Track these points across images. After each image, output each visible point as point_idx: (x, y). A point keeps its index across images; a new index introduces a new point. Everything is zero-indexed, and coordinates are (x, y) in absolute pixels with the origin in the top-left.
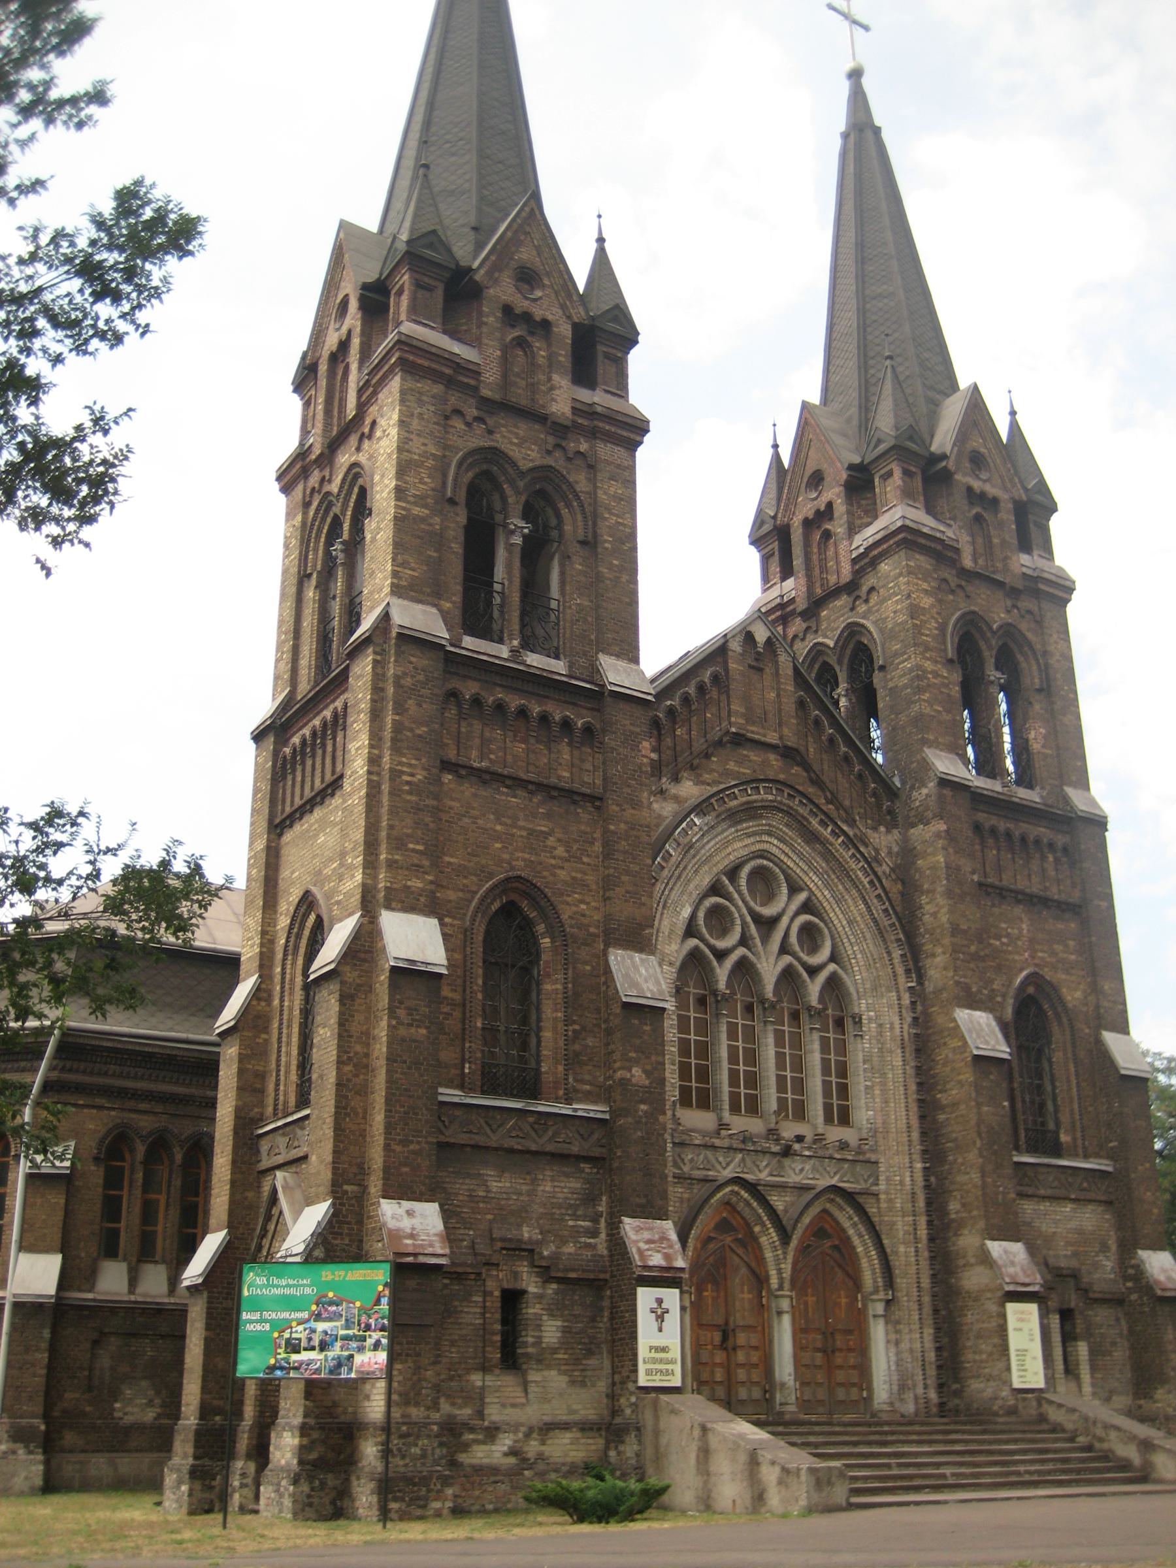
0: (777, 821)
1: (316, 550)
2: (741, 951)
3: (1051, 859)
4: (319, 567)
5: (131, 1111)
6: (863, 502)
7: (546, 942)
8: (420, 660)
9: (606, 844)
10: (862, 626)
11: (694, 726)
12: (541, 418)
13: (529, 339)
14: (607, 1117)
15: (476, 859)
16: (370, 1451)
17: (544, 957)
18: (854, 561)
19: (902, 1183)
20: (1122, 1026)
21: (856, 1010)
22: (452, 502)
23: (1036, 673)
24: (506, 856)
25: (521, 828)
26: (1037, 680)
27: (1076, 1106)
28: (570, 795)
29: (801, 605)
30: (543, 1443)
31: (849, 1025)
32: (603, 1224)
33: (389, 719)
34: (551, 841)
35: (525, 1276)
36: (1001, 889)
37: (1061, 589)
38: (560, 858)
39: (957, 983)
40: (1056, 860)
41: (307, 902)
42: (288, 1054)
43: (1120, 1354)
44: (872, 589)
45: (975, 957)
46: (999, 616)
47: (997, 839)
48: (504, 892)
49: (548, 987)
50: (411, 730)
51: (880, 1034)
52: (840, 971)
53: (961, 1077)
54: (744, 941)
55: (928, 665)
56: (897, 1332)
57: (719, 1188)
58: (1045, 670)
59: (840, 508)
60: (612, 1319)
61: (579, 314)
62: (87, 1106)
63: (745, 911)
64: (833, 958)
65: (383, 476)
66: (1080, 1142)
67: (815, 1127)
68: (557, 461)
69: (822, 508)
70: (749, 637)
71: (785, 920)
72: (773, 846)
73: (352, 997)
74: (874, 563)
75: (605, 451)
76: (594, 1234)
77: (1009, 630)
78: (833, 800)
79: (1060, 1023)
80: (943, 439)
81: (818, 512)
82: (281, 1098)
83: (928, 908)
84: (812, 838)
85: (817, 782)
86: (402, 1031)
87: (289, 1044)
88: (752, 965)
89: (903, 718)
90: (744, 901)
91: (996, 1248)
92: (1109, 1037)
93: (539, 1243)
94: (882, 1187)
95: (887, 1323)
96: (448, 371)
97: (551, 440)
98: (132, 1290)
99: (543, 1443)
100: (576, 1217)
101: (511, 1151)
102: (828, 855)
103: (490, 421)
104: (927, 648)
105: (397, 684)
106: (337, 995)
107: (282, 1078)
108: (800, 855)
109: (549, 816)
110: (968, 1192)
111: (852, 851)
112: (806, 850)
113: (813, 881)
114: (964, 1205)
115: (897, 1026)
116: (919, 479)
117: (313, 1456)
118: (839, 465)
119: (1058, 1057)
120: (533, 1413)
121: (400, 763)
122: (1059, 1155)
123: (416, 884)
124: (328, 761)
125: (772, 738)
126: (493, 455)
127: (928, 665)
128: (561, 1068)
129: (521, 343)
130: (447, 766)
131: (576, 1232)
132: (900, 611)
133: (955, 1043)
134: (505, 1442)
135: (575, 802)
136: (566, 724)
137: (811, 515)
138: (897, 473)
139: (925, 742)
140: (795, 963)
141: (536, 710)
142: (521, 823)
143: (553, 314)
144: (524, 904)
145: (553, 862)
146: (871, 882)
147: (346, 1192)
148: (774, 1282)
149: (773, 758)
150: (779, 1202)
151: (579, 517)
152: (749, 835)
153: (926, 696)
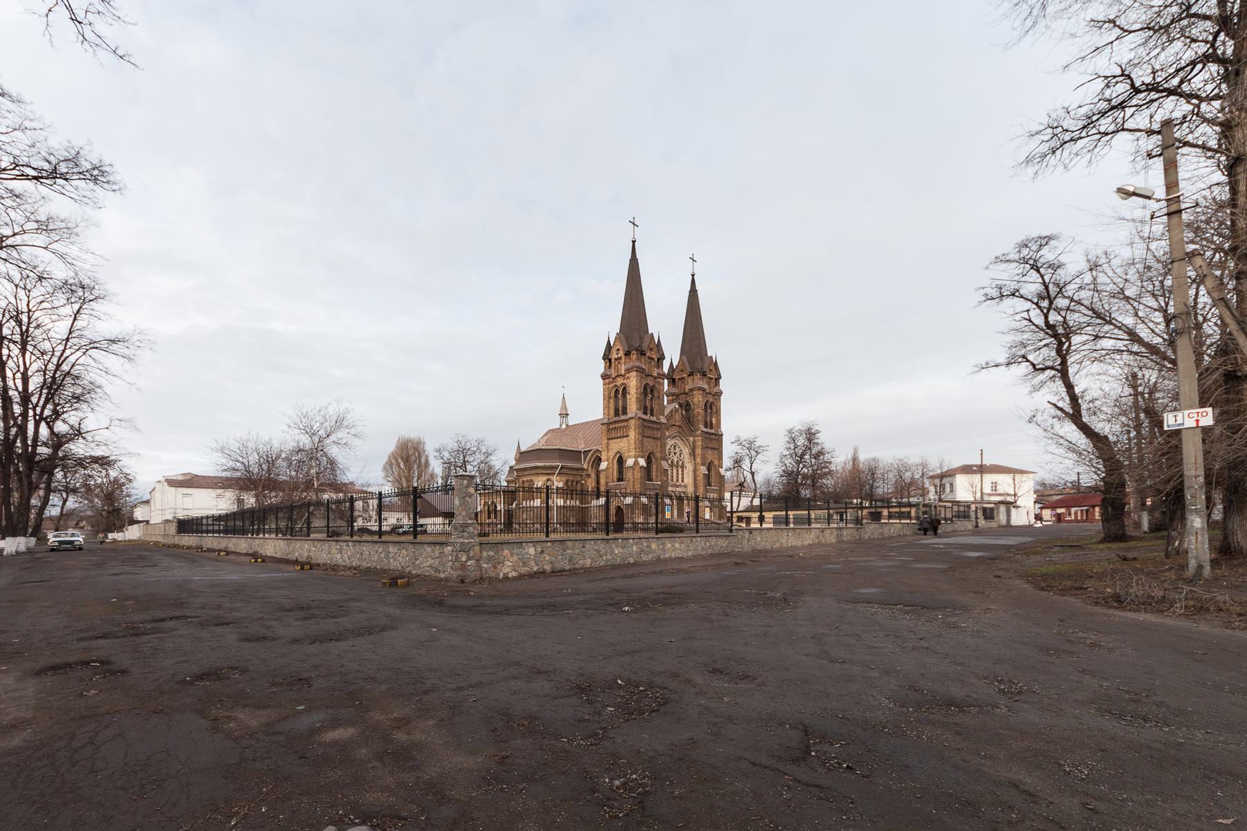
0: (678, 438)
28: (657, 439)
41: (618, 452)
61: (658, 357)
84: (682, 440)
113: (682, 446)
125: (677, 424)
143: (654, 356)
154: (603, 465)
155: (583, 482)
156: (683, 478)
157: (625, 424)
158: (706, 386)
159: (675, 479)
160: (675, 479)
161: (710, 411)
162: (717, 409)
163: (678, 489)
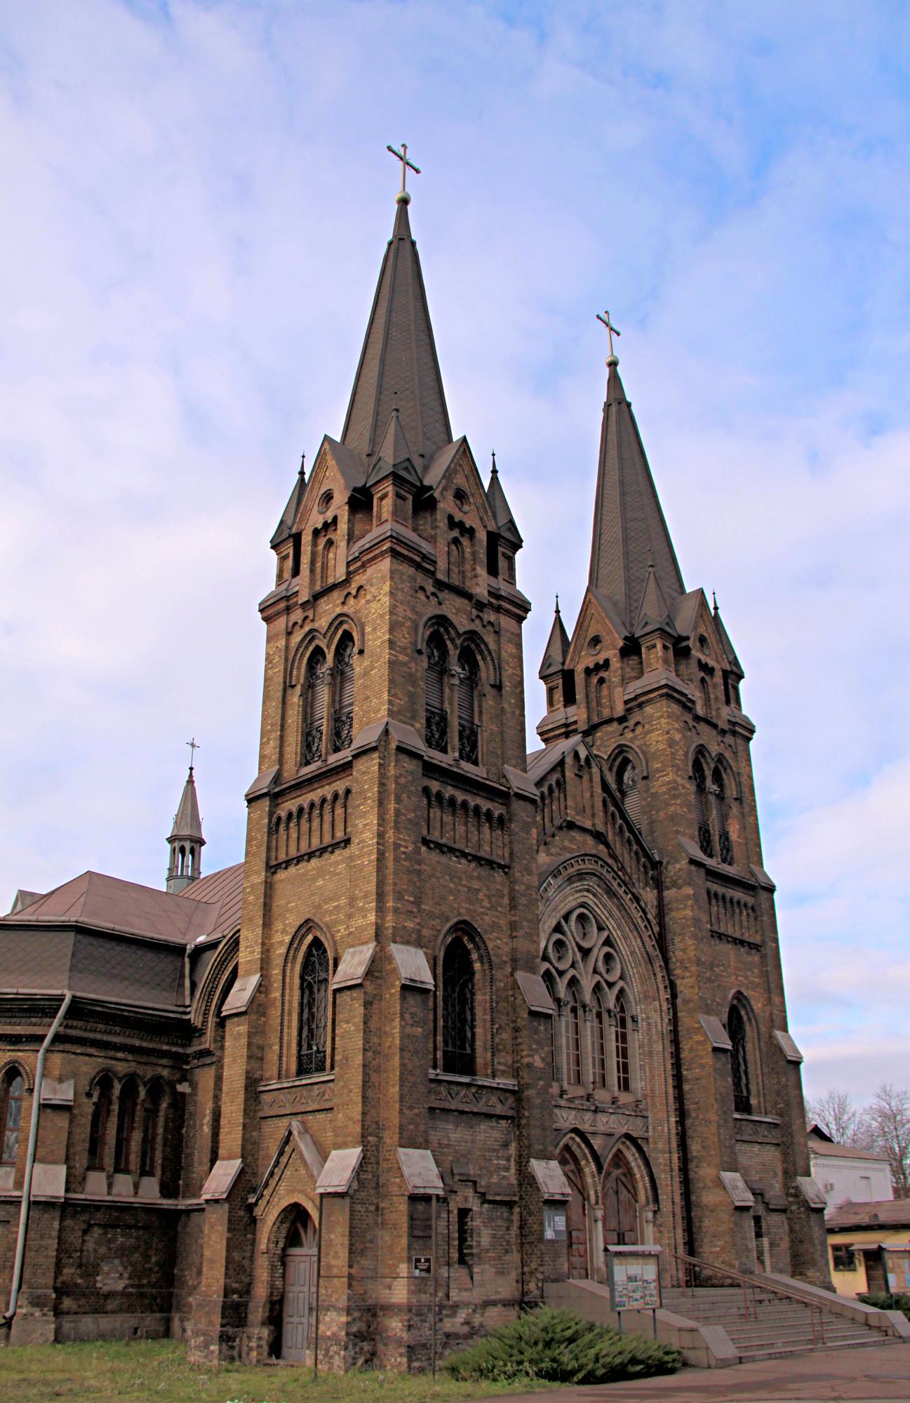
0: (592, 882)
1: (299, 669)
2: (571, 972)
3: (745, 913)
4: (302, 681)
5: (112, 1058)
6: (631, 662)
7: (477, 966)
8: (411, 766)
9: (512, 899)
10: (631, 748)
11: (546, 815)
12: (468, 596)
13: (461, 539)
14: (516, 1088)
15: (438, 907)
16: (395, 1325)
17: (478, 976)
18: (626, 702)
19: (662, 1131)
20: (785, 1028)
21: (634, 1013)
22: (420, 652)
23: (734, 787)
24: (456, 906)
25: (465, 886)
26: (735, 792)
27: (760, 1080)
28: (491, 864)
29: (582, 726)
30: (482, 1315)
31: (629, 1021)
32: (513, 1162)
33: (392, 806)
34: (481, 896)
35: (471, 1199)
36: (721, 934)
37: (744, 731)
38: (487, 908)
39: (700, 998)
40: (748, 914)
41: (307, 925)
42: (289, 1034)
43: (785, 1245)
44: (637, 723)
45: (709, 980)
46: (714, 749)
47: (717, 900)
48: (456, 931)
49: (479, 997)
50: (405, 815)
51: (649, 1029)
52: (626, 987)
53: (703, 1061)
54: (573, 966)
55: (679, 779)
56: (660, 1232)
57: (565, 1135)
58: (739, 785)
59: (615, 663)
60: (521, 1227)
61: (492, 527)
62: (81, 1054)
63: (574, 944)
64: (621, 978)
65: (374, 629)
66: (762, 1104)
67: (613, 1092)
68: (477, 626)
69: (601, 662)
70: (576, 755)
71: (595, 951)
72: (590, 899)
73: (371, 1003)
74: (640, 706)
75: (506, 622)
76: (507, 1169)
77: (720, 759)
78: (622, 868)
79: (751, 1025)
80: (683, 626)
81: (597, 665)
82: (284, 1066)
83: (680, 945)
84: (611, 894)
85: (613, 856)
86: (408, 1030)
87: (289, 1027)
88: (578, 981)
89: (662, 814)
90: (574, 939)
91: (727, 1176)
92: (778, 1034)
93: (480, 1176)
94: (651, 1134)
95: (654, 1225)
96: (418, 559)
97: (475, 612)
98: (109, 1194)
99: (482, 1315)
100: (498, 1158)
101: (462, 1112)
102: (621, 907)
103: (440, 595)
104: (679, 769)
105: (397, 783)
106: (362, 1002)
107: (285, 1051)
108: (605, 906)
109: (479, 878)
110: (706, 1138)
111: (635, 905)
112: (609, 903)
113: (611, 924)
114: (703, 1147)
115: (659, 1024)
116: (671, 651)
117: (354, 1329)
118: (616, 635)
119: (749, 1047)
120: (476, 1296)
121: (400, 839)
122: (750, 1113)
123: (410, 924)
124: (327, 826)
125: (588, 824)
126: (441, 621)
127: (679, 779)
128: (489, 1054)
129: (456, 541)
130: (425, 842)
131: (498, 1168)
132: (662, 742)
133: (699, 1038)
134: (462, 1315)
135: (493, 869)
136: (489, 814)
137: (591, 666)
138: (659, 646)
139: (678, 832)
140: (602, 981)
141: (472, 804)
142: (464, 882)
144: (465, 939)
145: (482, 910)
146: (646, 927)
147: (369, 1142)
148: (593, 1198)
149: (590, 840)
150: (597, 1143)
151: (491, 668)
152: (577, 892)
153: (678, 801)
154: (240, 996)
155: (183, 1088)
156: (624, 1068)
157: (340, 786)
158: (693, 692)
159: (590, 1073)
160: (590, 1073)
161: (715, 788)
162: (739, 785)
163: (605, 1122)
